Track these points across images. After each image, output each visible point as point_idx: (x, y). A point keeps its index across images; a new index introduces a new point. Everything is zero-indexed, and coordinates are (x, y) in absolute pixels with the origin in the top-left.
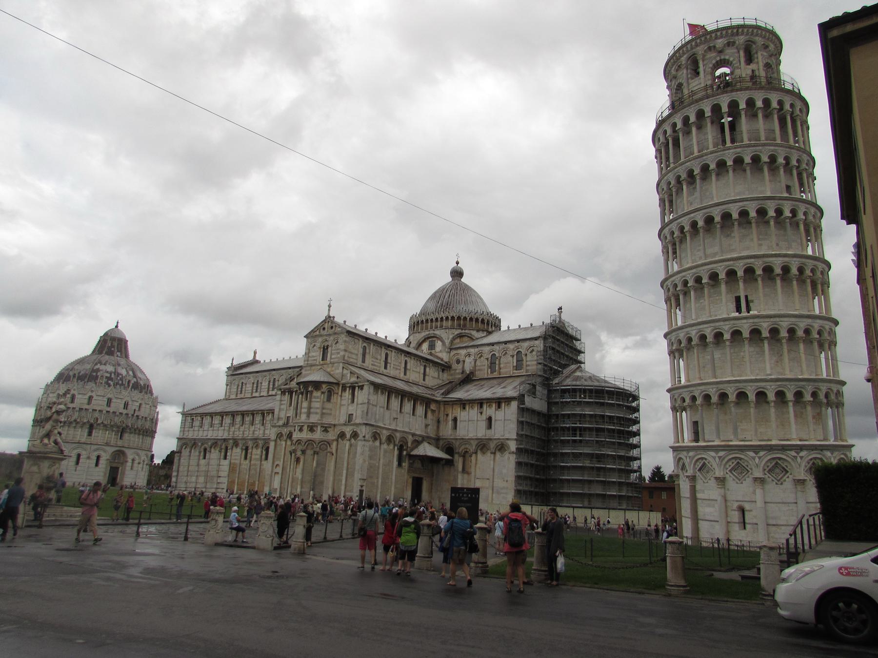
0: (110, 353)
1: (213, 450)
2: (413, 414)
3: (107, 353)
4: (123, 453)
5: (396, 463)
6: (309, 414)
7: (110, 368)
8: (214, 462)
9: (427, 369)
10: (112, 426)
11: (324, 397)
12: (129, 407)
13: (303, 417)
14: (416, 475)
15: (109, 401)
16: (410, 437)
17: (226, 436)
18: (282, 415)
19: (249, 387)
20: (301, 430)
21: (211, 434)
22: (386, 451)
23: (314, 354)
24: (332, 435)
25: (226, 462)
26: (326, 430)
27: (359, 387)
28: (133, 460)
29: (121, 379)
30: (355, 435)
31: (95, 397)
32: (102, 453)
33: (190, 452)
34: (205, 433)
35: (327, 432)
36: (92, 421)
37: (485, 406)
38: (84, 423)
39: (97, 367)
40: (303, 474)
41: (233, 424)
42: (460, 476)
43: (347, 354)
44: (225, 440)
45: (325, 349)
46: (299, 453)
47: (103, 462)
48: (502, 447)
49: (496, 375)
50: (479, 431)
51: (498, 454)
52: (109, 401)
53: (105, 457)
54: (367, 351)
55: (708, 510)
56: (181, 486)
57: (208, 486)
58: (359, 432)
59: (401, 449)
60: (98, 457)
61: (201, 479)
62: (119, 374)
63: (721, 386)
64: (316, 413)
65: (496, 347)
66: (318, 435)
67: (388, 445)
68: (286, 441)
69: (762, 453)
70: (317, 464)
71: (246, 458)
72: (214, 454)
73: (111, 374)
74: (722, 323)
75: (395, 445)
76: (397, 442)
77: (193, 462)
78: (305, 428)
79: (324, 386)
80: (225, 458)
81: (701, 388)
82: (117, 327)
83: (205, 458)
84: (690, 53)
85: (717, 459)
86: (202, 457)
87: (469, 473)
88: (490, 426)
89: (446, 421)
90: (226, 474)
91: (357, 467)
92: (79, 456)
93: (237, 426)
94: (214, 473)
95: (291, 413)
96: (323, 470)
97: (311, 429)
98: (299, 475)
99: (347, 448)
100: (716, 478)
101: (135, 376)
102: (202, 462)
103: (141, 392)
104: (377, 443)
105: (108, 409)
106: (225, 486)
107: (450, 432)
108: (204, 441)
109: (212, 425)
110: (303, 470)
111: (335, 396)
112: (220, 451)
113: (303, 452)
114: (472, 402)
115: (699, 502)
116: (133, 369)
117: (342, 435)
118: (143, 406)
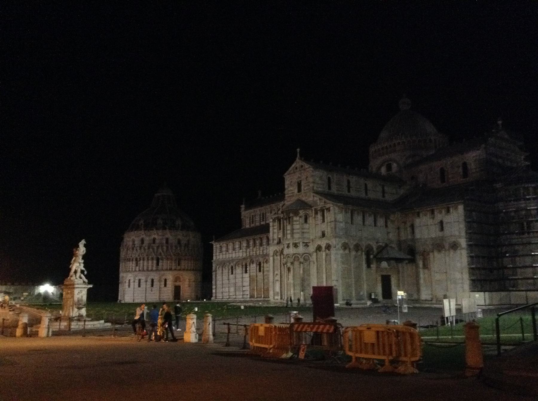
2: (375, 226)
5: (364, 266)
6: (292, 234)
8: (239, 276)
9: (386, 188)
11: (302, 220)
13: (289, 236)
14: (384, 274)
16: (375, 243)
18: (276, 237)
19: (257, 218)
20: (288, 247)
22: (356, 257)
23: (291, 188)
24: (312, 248)
25: (247, 275)
26: (306, 245)
27: (327, 209)
30: (328, 247)
32: (167, 277)
34: (231, 256)
35: (308, 246)
40: (294, 279)
42: (421, 271)
43: (315, 186)
45: (299, 185)
46: (289, 264)
47: (168, 282)
50: (434, 233)
51: (452, 252)
54: (332, 180)
56: (219, 296)
57: (237, 293)
58: (331, 243)
59: (368, 254)
61: (232, 289)
64: (298, 233)
66: (301, 249)
67: (357, 251)
68: (280, 255)
70: (304, 271)
71: (260, 271)
72: (239, 270)
75: (362, 252)
76: (364, 249)
77: (225, 278)
78: (291, 245)
79: (301, 212)
80: (246, 272)
83: (232, 274)
86: (230, 273)
87: (427, 268)
88: (442, 229)
89: (406, 229)
90: (248, 284)
91: (333, 271)
93: (251, 248)
94: (240, 284)
95: (280, 236)
96: (309, 275)
97: (296, 245)
98: (291, 281)
99: (324, 257)
102: (231, 276)
104: (347, 251)
106: (248, 293)
107: (410, 237)
109: (234, 249)
110: (294, 276)
111: (310, 218)
113: (292, 263)
117: (319, 248)
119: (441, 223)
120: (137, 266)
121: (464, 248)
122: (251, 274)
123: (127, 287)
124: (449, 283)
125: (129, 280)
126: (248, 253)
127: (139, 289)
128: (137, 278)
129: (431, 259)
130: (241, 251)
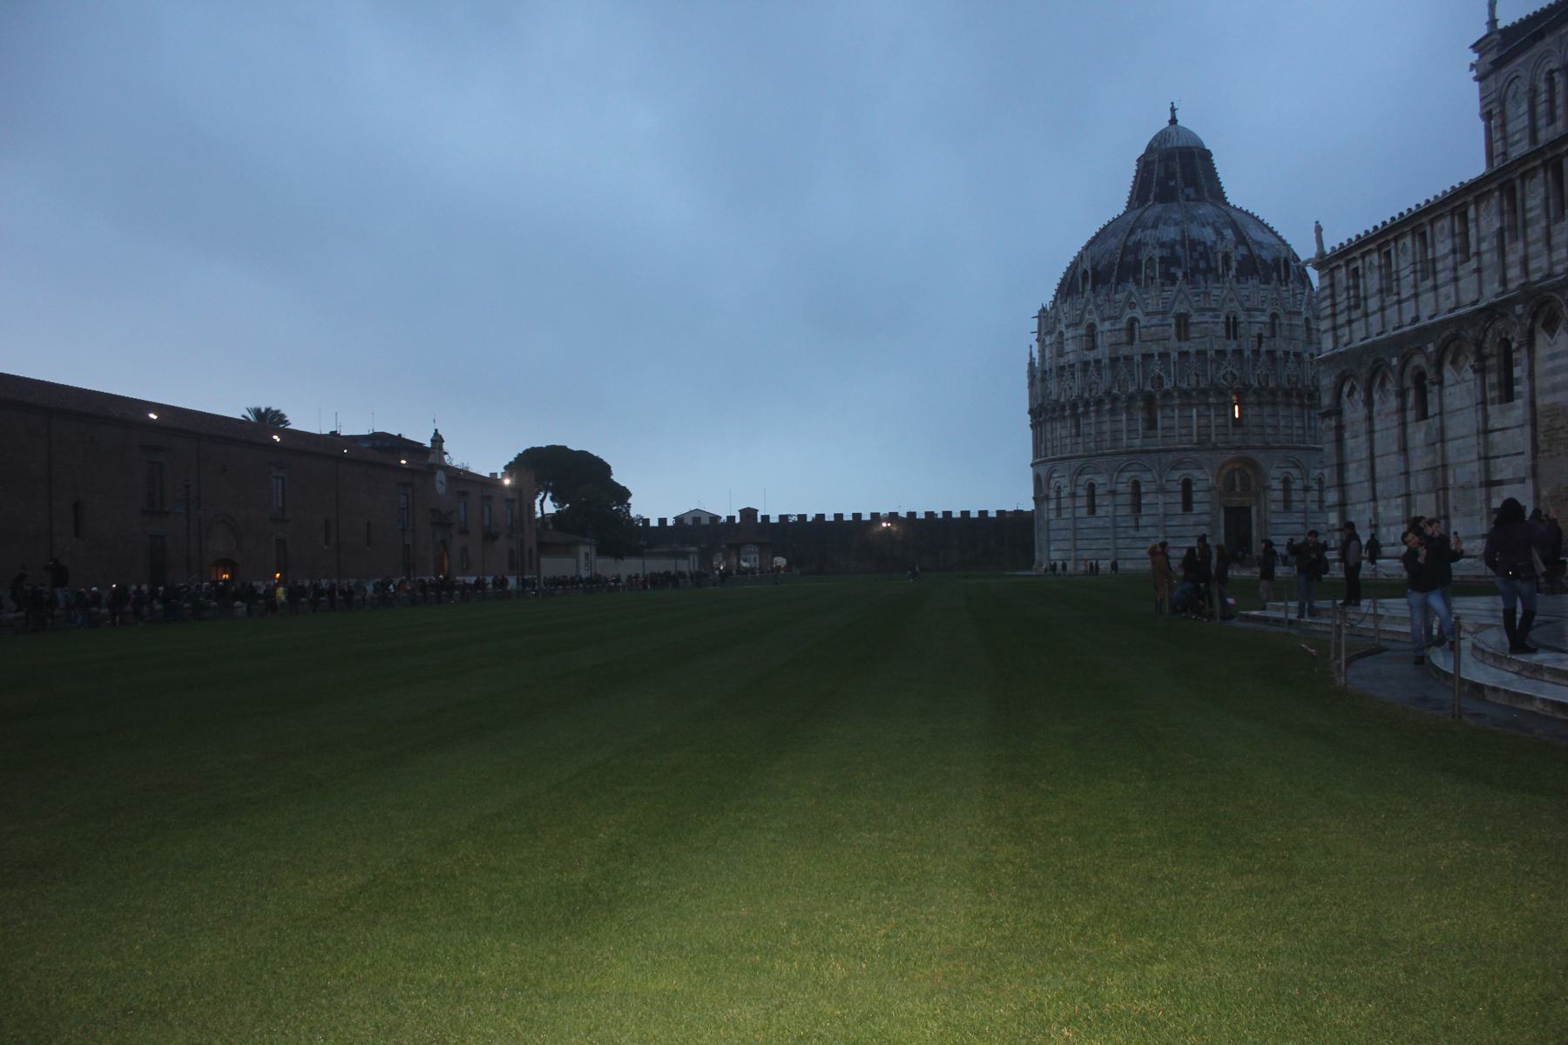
0: (1166, 196)
1: (1448, 373)
3: (1161, 199)
4: (1252, 464)
7: (1170, 233)
8: (1463, 425)
10: (1204, 392)
12: (1241, 330)
15: (1183, 322)
17: (1492, 291)
21: (1430, 307)
28: (1286, 482)
29: (1205, 256)
31: (1143, 321)
32: (1196, 474)
33: (1369, 403)
36: (1148, 388)
38: (1131, 398)
39: (1134, 238)
41: (1513, 228)
44: (1491, 313)
52: (1183, 322)
53: (1204, 479)
60: (1187, 485)
62: (1194, 244)
72: (1459, 390)
73: (1172, 245)
80: (1508, 396)
82: (1173, 121)
83: (1423, 415)
86: (1411, 415)
90: (1524, 462)
92: (1136, 485)
93: (1535, 232)
101: (1241, 239)
102: (1418, 434)
103: (1267, 282)
105: (1185, 346)
108: (1405, 344)
109: (1427, 268)
112: (1481, 371)
116: (1240, 224)
118: (1284, 320)
120: (1078, 435)
122: (1543, 401)
123: (1052, 515)
125: (1059, 490)
126: (1514, 272)
127: (1094, 522)
128: (1083, 479)
130: (1473, 264)
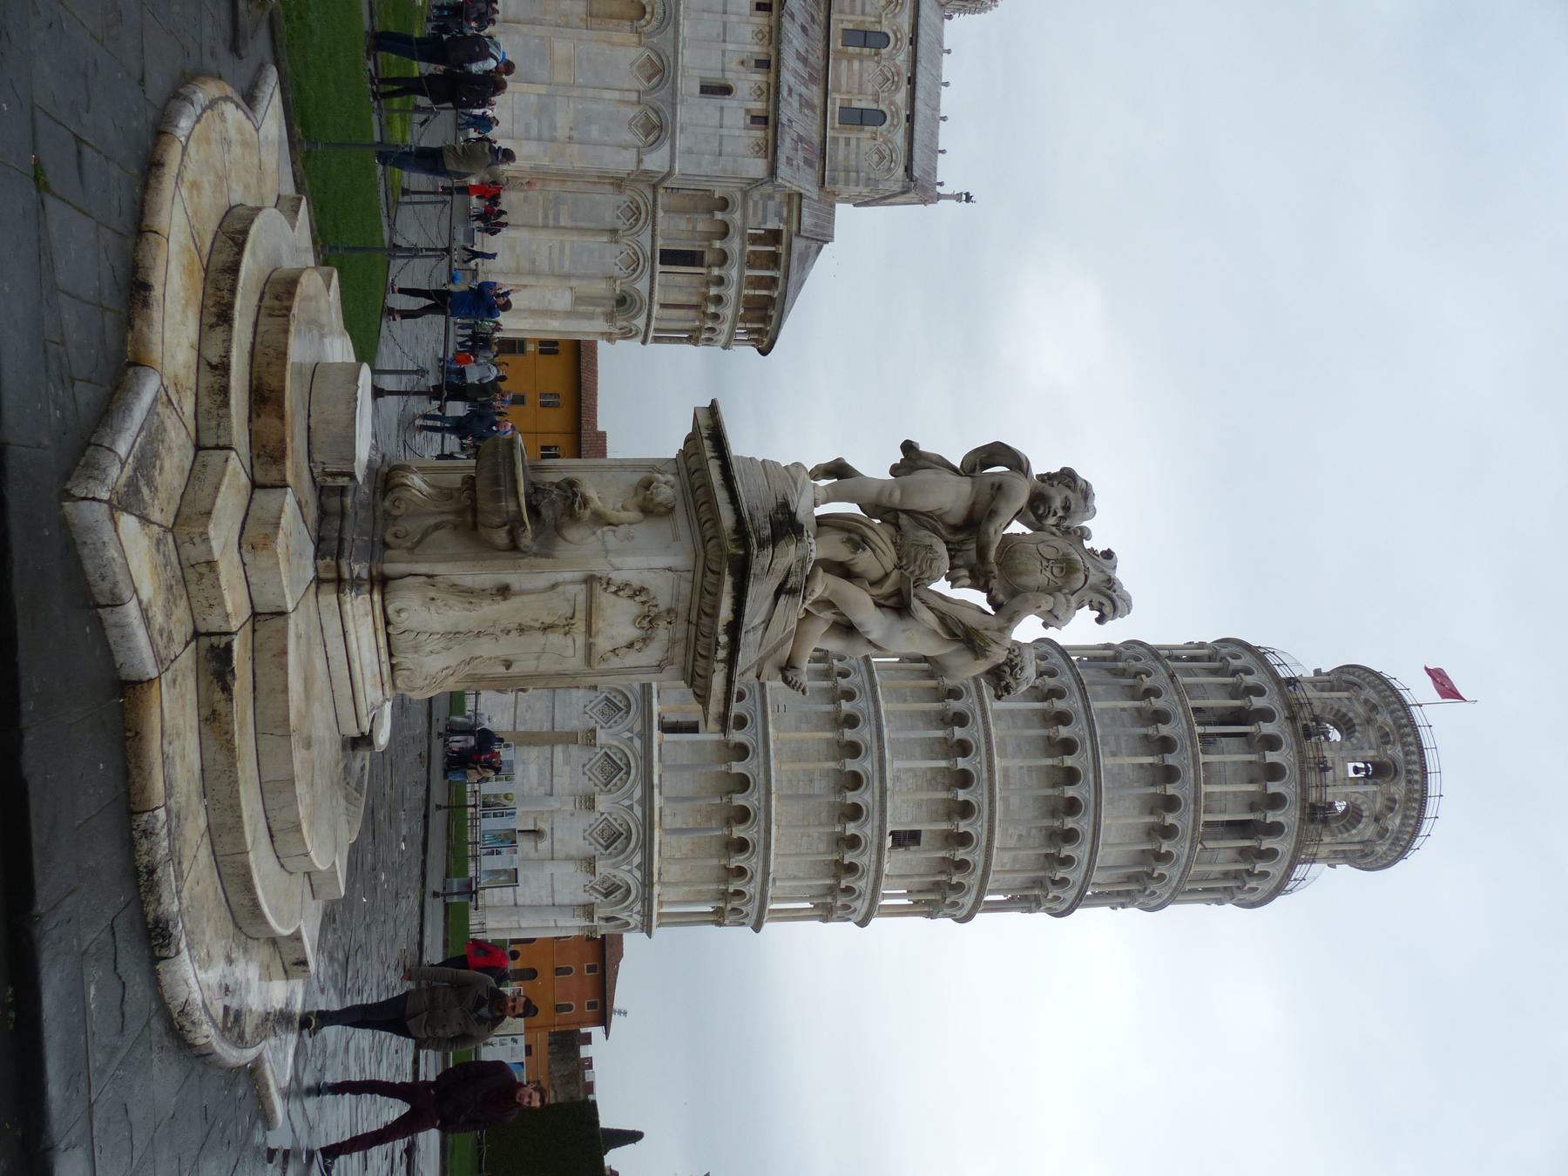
37: (758, 78)
48: (657, 128)
49: (836, 43)
50: (694, 64)
55: (533, 769)
63: (762, 816)
65: (906, 47)
69: (638, 874)
74: (876, 823)
81: (762, 775)
84: (1401, 765)
85: (627, 802)
88: (709, 89)
100: (594, 731)
114: (774, 37)
115: (547, 749)
119: (726, 90)
121: (640, 161)
124: (543, 89)
129: (617, 37)
